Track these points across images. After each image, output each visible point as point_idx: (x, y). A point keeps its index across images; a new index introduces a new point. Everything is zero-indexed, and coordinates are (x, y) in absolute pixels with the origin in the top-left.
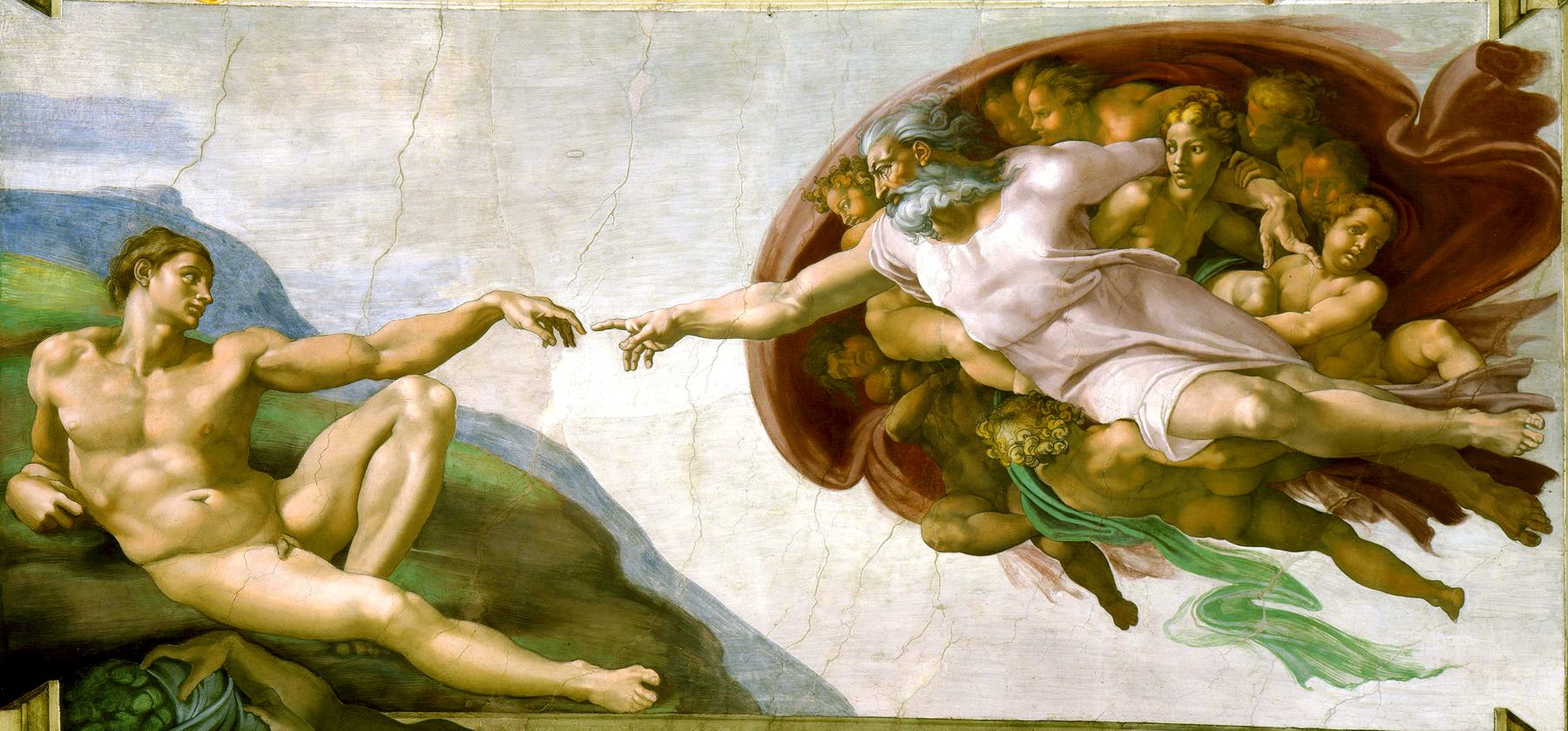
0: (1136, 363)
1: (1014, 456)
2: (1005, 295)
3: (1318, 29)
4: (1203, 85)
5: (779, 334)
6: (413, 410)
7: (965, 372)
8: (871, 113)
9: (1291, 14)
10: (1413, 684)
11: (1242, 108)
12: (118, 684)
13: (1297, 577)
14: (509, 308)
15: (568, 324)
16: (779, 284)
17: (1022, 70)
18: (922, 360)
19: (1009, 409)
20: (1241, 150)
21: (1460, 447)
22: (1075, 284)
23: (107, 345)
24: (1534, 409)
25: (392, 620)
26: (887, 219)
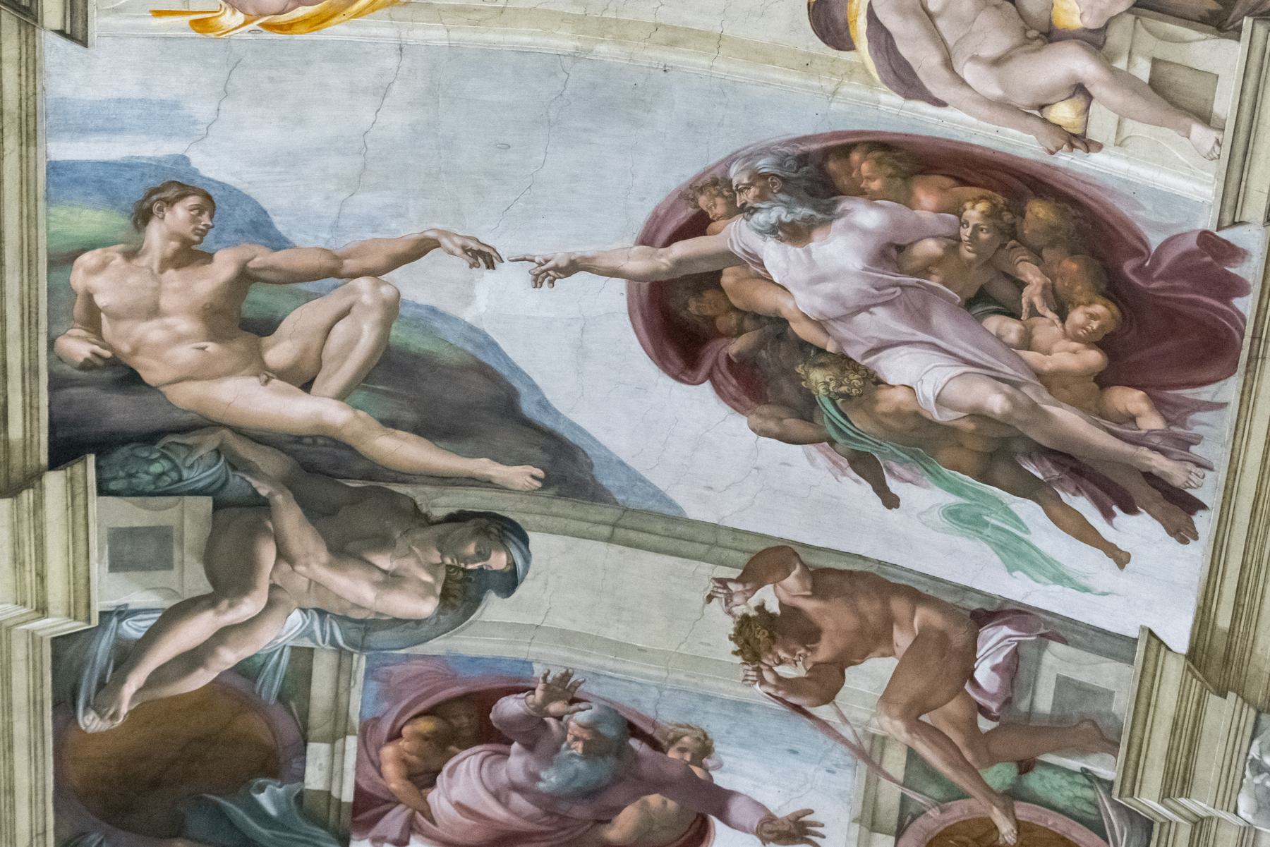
0: (918, 353)
1: (821, 389)
2: (828, 287)
3: (1083, 182)
4: (995, 191)
5: (654, 280)
6: (367, 299)
7: (793, 332)
8: (739, 151)
9: (1066, 166)
10: (1087, 595)
11: (1022, 214)
12: (137, 457)
13: (1017, 512)
14: (444, 241)
15: (489, 255)
16: (655, 249)
17: (859, 148)
18: (761, 314)
19: (822, 360)
20: (1016, 239)
21: (1143, 470)
22: (881, 292)
23: (131, 255)
24: (1199, 465)
25: (344, 425)
26: (744, 222)
